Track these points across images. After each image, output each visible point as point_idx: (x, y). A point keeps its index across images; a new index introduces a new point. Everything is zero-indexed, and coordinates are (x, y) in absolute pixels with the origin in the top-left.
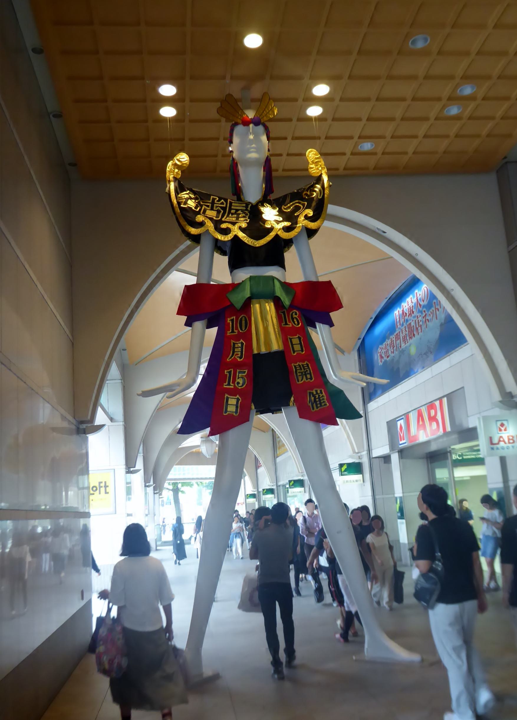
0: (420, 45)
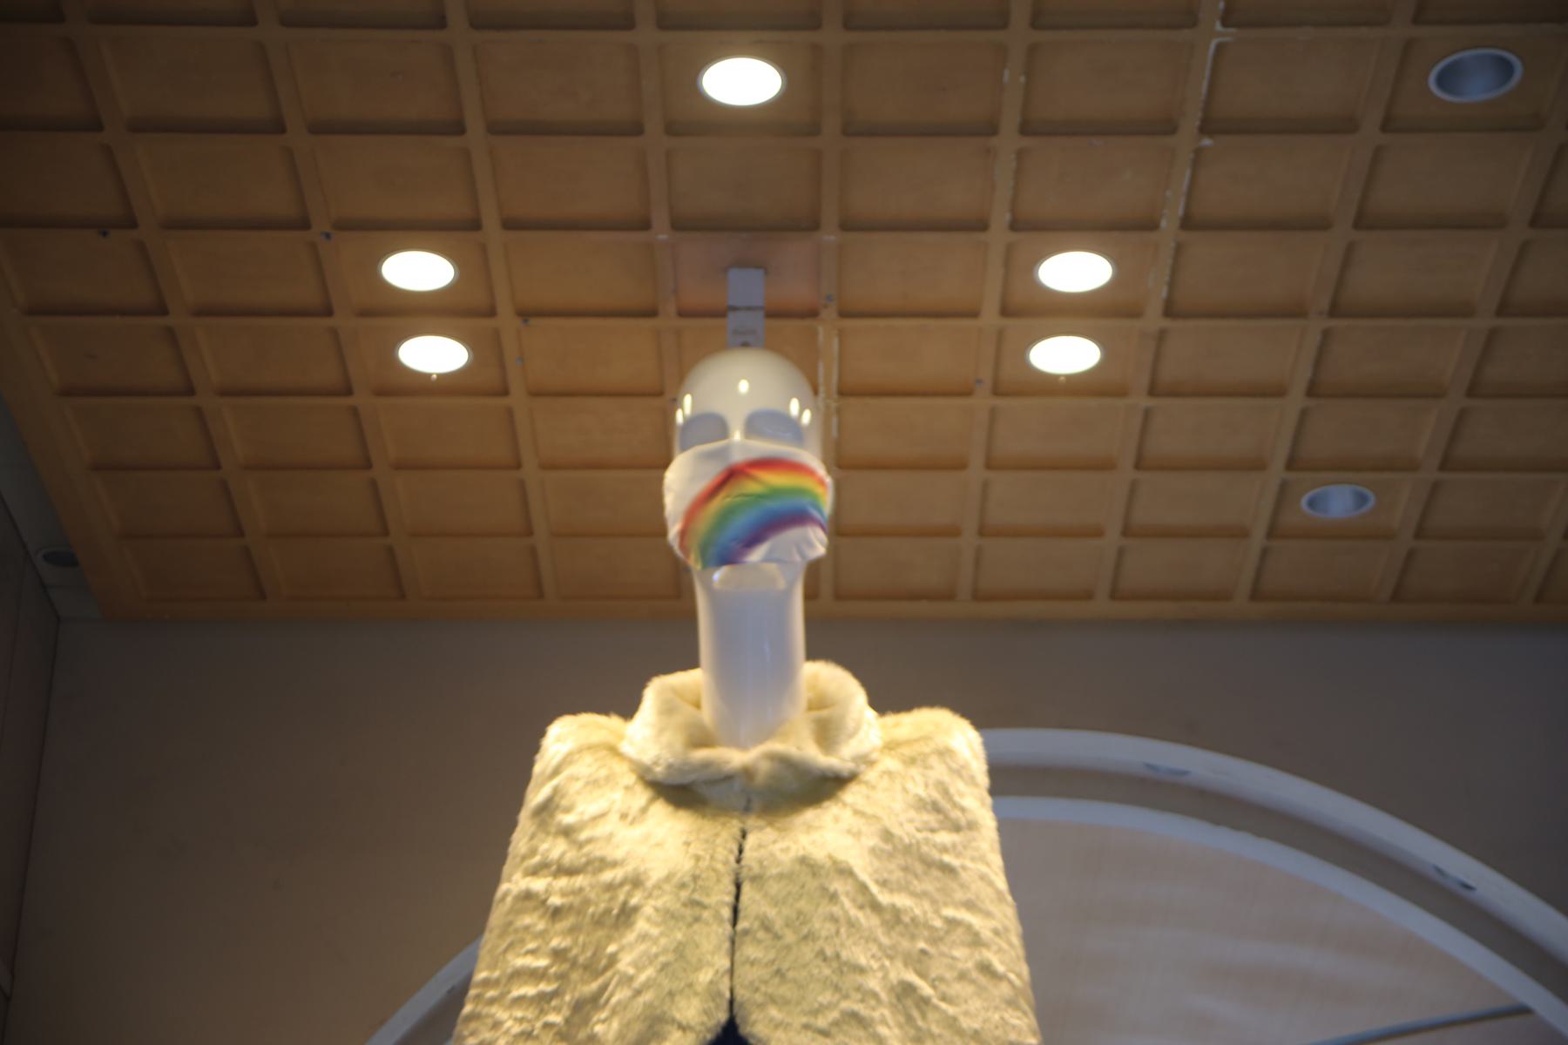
0: (1477, 92)
